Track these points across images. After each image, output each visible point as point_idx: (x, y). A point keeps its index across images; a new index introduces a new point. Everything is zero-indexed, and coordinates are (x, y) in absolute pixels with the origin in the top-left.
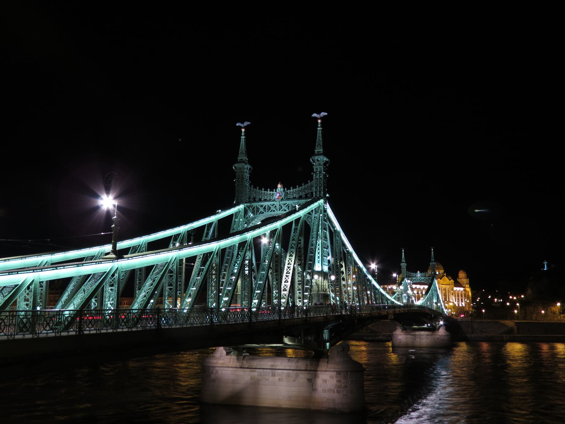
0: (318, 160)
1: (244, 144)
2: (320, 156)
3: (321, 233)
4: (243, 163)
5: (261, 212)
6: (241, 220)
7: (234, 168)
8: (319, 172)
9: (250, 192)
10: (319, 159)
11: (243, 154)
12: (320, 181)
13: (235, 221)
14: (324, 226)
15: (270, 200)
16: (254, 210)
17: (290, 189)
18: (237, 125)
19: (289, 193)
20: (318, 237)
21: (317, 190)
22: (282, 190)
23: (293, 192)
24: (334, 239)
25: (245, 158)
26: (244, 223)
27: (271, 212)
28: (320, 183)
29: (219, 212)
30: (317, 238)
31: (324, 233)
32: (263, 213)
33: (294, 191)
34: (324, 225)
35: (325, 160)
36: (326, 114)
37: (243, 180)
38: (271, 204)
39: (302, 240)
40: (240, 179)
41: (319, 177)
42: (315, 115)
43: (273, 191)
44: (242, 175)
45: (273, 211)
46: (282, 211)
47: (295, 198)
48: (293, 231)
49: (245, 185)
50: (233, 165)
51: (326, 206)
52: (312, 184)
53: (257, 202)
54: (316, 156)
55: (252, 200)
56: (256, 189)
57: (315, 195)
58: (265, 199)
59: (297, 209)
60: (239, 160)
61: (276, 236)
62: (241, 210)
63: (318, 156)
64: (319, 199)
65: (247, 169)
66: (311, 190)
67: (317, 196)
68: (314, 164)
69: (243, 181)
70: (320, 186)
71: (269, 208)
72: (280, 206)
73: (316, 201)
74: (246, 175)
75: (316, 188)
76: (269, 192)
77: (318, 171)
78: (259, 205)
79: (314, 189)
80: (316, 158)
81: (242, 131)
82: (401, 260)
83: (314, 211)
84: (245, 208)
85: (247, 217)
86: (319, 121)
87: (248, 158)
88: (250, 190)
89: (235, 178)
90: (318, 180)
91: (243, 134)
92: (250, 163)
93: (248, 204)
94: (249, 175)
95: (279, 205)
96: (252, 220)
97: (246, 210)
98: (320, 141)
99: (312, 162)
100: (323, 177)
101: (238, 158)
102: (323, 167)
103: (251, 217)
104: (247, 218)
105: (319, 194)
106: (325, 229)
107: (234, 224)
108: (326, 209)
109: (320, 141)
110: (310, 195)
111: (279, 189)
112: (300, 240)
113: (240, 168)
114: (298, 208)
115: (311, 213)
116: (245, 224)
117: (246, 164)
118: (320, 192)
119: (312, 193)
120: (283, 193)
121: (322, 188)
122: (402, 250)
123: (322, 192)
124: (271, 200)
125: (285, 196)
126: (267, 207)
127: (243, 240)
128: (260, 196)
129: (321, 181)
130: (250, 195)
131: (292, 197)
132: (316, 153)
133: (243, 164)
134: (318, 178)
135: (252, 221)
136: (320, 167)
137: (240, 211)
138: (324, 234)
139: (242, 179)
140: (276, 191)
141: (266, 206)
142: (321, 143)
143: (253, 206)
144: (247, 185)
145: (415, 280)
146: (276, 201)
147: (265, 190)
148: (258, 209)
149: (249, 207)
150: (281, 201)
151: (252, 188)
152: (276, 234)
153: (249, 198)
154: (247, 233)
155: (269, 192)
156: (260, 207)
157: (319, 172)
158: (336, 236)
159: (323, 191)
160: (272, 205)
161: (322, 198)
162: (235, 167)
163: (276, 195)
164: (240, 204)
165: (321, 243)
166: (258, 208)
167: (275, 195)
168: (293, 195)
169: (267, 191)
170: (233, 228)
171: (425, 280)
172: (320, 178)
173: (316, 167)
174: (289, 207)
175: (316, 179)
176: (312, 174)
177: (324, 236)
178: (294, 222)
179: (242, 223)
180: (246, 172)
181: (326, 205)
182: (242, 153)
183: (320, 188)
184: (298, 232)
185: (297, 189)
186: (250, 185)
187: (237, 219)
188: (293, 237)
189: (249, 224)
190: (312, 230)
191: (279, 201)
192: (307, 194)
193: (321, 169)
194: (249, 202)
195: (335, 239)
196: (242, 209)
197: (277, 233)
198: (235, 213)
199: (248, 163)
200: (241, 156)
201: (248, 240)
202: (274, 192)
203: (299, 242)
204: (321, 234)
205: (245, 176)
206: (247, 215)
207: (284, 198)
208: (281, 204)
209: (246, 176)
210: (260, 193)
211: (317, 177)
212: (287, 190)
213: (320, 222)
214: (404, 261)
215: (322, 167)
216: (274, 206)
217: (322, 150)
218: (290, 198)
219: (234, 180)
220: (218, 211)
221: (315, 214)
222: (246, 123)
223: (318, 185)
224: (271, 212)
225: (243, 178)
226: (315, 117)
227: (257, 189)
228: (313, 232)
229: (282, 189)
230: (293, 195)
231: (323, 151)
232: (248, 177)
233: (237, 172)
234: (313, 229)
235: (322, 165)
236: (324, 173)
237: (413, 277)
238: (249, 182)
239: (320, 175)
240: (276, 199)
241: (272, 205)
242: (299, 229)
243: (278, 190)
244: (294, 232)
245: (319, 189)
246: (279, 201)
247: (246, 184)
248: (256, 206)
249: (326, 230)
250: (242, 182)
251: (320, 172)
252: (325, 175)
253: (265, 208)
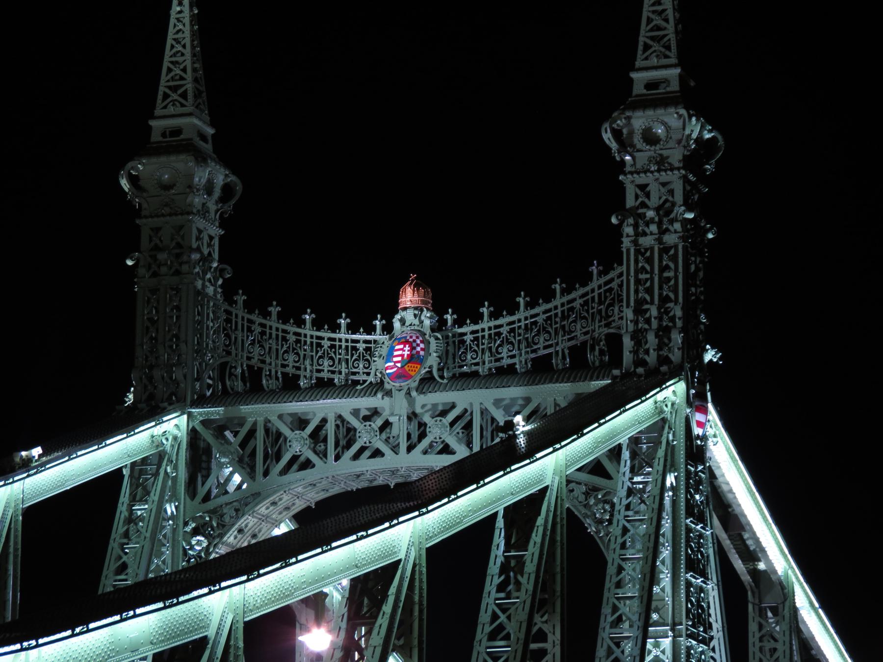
0: (650, 138)
1: (187, 34)
2: (660, 111)
3: (668, 590)
4: (182, 157)
5: (295, 458)
6: (170, 509)
7: (124, 184)
8: (657, 209)
9: (228, 336)
10: (660, 131)
11: (184, 95)
12: (663, 269)
13: (131, 519)
14: (688, 545)
15: (351, 387)
16: (249, 449)
17: (477, 318)
19: (468, 338)
20: (655, 616)
21: (648, 321)
22: (427, 322)
23: (499, 334)
24: (753, 627)
25: (196, 121)
26: (188, 529)
27: (356, 457)
28: (664, 281)
29: (30, 459)
30: (647, 622)
31: (688, 592)
32: (307, 465)
33: (504, 330)
34: (688, 540)
35: (695, 135)
37: (181, 264)
38: (356, 413)
39: (550, 637)
40: (162, 256)
41: (660, 241)
43: (370, 330)
44: (181, 227)
45: (367, 453)
46: (425, 452)
47: (511, 369)
48: (497, 581)
49: (198, 293)
50: (122, 166)
51: (700, 425)
52: (614, 285)
53: (273, 396)
54: (639, 113)
55: (239, 386)
56: (266, 315)
57: (635, 352)
58: (320, 380)
59: (521, 441)
60: (156, 137)
61: (387, 608)
62: (168, 445)
63: (650, 113)
64: (659, 382)
65: (209, 189)
66: (608, 325)
67: (642, 363)
68: (623, 162)
69: (185, 268)
70: (664, 300)
71: (347, 436)
72: (414, 423)
73: (640, 393)
74: (200, 231)
75: (639, 311)
76: (343, 336)
77: (654, 201)
78: (280, 417)
79: (629, 314)
80: (639, 121)
83: (626, 455)
84: (193, 434)
85: (209, 492)
87: (212, 124)
88: (228, 321)
89: (133, 247)
90: (649, 261)
93: (216, 412)
94: (221, 226)
95: (409, 419)
96: (239, 513)
97: (202, 445)
98: (666, 20)
99: (614, 145)
100: (684, 239)
101: (152, 123)
102: (685, 178)
103: (231, 488)
104: (207, 498)
105: (660, 348)
106: (696, 566)
107: (126, 535)
108: (704, 438)
109: (666, 20)
110: (602, 352)
111: (409, 316)
112: (541, 636)
113: (167, 187)
114: (528, 434)
115: (608, 466)
116: (196, 532)
117: (201, 158)
118: (664, 333)
119: (615, 341)
120: (432, 341)
121: (678, 312)
123: (677, 338)
124: (356, 383)
125: (444, 357)
126: (330, 428)
127: (183, 633)
128: (291, 358)
129: (667, 267)
130: (229, 353)
131: (487, 365)
132: (638, 89)
133: (182, 163)
134: (652, 249)
135: (238, 518)
136: (664, 177)
137: (161, 456)
138: (688, 600)
139: (178, 256)
140: (388, 329)
141: (324, 421)
142: (670, 28)
143: (242, 425)
144: (210, 290)
146: (389, 393)
147: (317, 325)
148: (276, 439)
149: (219, 428)
150: (420, 389)
151: (239, 311)
152: (391, 599)
153: (223, 370)
154: (205, 590)
155: (343, 336)
156: (285, 431)
157: (657, 209)
158: (762, 613)
159: (683, 330)
160: (364, 413)
161: (675, 373)
162: (134, 180)
163: (390, 356)
164: (164, 412)
165: (669, 652)
166: (279, 434)
167: (384, 351)
168: (495, 354)
169: (335, 328)
170: (120, 558)
172: (665, 250)
173: (641, 179)
174: (468, 426)
175: (638, 252)
176: (614, 220)
177: (688, 611)
178: (500, 523)
179: (174, 531)
180: (204, 212)
181: (699, 417)
182: (174, 89)
183: (664, 311)
184: (527, 582)
185: (521, 314)
186: (229, 291)
187: (143, 501)
188: (495, 617)
189: (221, 536)
190: (611, 570)
191: (408, 393)
192: (584, 343)
193: (671, 192)
194: (223, 396)
195: (761, 627)
196: (175, 438)
197: (393, 590)
198: (133, 464)
199: (215, 150)
200: (171, 110)
201: (211, 633)
202: (377, 336)
203: (533, 646)
204: (669, 600)
205: (195, 232)
206: (206, 477)
207: (440, 370)
208: (418, 410)
209: (198, 238)
210: (292, 338)
211: (646, 241)
212: (459, 322)
213: (667, 525)
215: (675, 179)
216: (379, 422)
217: (678, 71)
218: (475, 374)
219: (130, 263)
220: (24, 453)
221: (634, 471)
223: (649, 291)
224: (356, 457)
225: (181, 249)
227: (270, 314)
228: (619, 585)
229: (427, 314)
230: (495, 354)
231: (680, 76)
232: (216, 242)
233: (144, 213)
234: (620, 569)
235: (677, 165)
236: (690, 216)
238: (221, 272)
239: (663, 232)
240: (387, 380)
241: (366, 418)
242: (530, 567)
243: (403, 321)
244: (501, 588)
245: (660, 318)
246: (408, 393)
247: (199, 284)
248: (267, 421)
249: (703, 574)
250: (177, 273)
251: (665, 210)
252: (692, 230)
253: (317, 436)
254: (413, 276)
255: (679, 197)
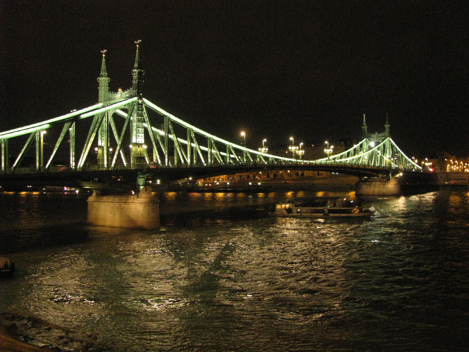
36: (141, 41)
86: (138, 46)
91: (103, 58)
92: (109, 76)
161: (136, 96)
222: (105, 51)
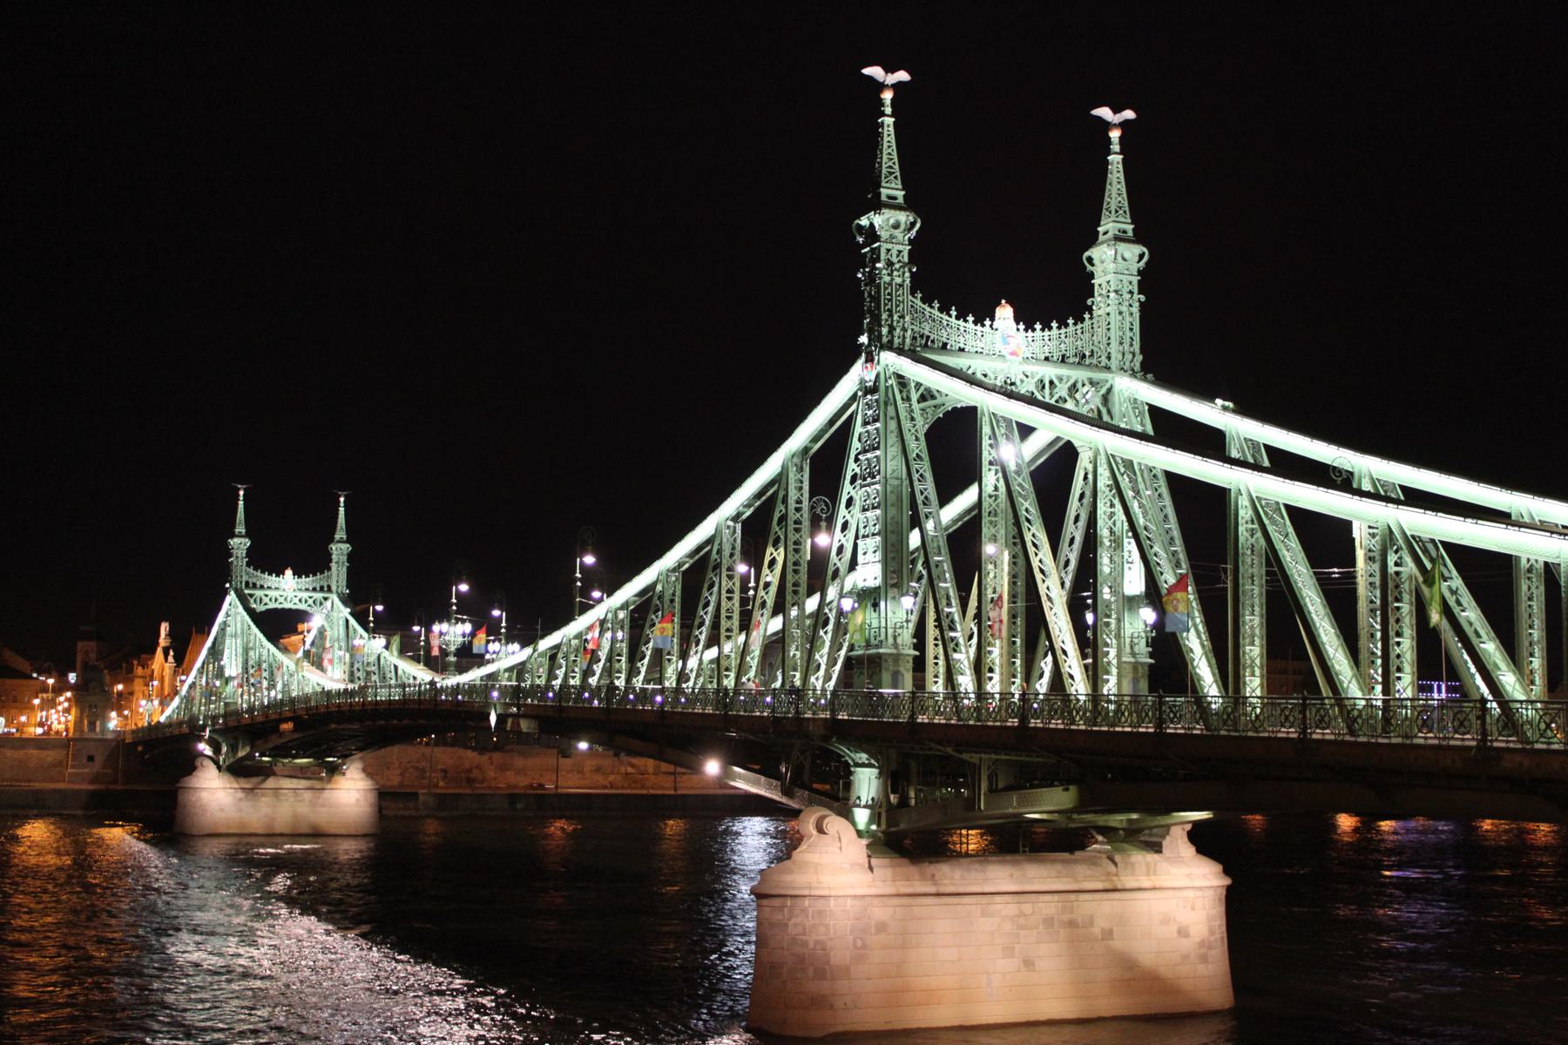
0: (1124, 259)
10: (1127, 255)
11: (896, 178)
18: (867, 71)
42: (1104, 112)
43: (983, 325)
81: (881, 103)
82: (233, 525)
122: (239, 489)
140: (991, 326)
145: (276, 600)
171: (310, 601)
182: (891, 173)
211: (1124, 309)
214: (244, 531)
215: (1135, 280)
217: (1132, 226)
222: (903, 76)
226: (1100, 121)
237: (269, 588)
254: (1003, 301)
255: (1136, 290)
